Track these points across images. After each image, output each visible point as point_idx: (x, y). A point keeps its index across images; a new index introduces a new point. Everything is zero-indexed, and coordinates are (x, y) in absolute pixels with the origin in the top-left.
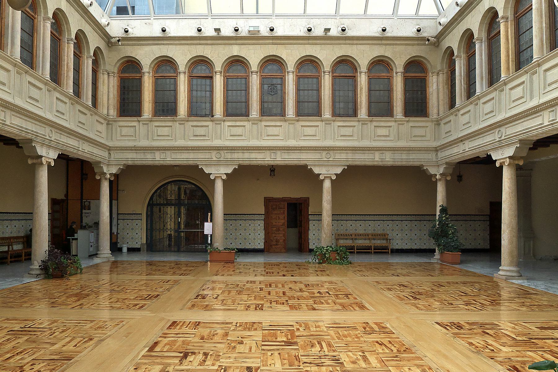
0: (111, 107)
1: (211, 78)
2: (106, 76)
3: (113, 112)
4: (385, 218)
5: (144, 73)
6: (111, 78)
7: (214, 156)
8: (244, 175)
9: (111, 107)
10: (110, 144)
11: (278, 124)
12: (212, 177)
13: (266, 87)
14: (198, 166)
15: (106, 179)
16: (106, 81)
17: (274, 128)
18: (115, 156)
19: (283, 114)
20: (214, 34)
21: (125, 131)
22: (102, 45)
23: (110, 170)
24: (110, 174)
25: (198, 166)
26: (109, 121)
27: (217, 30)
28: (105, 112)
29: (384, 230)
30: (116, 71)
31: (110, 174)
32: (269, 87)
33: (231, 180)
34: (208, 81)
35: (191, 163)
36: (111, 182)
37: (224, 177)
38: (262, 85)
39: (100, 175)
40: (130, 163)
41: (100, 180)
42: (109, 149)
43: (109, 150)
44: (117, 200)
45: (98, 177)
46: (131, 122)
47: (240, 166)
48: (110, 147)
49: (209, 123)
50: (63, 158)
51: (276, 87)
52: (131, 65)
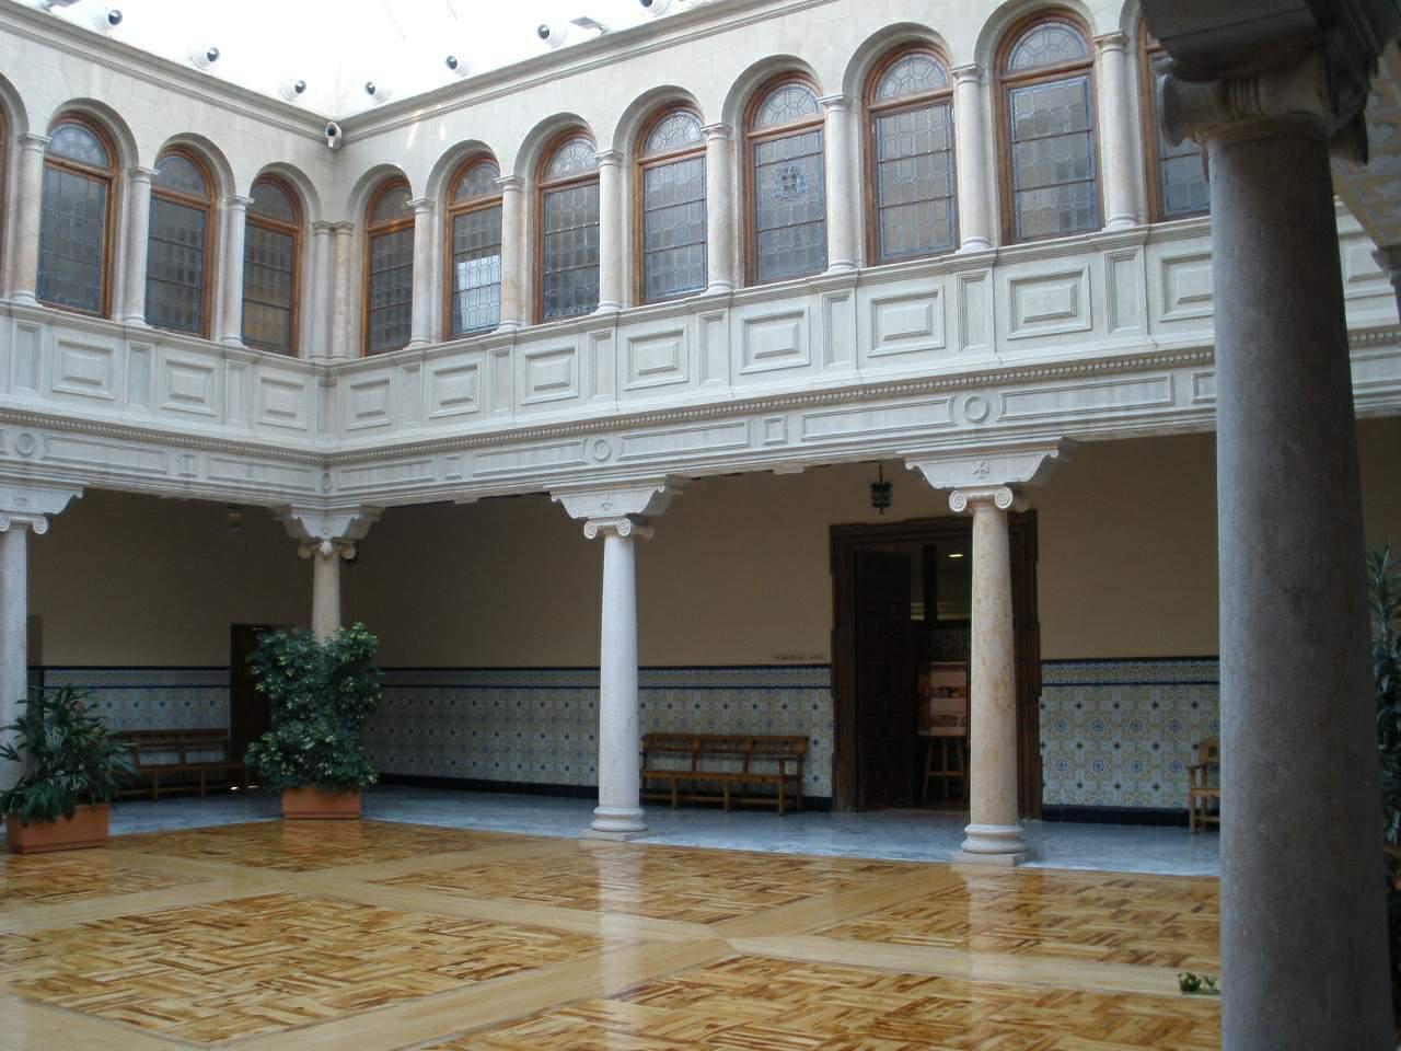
2: (324, 238)
4: (690, 678)
6: (343, 239)
8: (702, 517)
12: (590, 532)
18: (342, 481)
23: (326, 530)
24: (335, 541)
29: (656, 722)
36: (345, 564)
37: (626, 528)
40: (385, 501)
41: (312, 558)
45: (305, 553)
49: (579, 342)
52: (389, 184)
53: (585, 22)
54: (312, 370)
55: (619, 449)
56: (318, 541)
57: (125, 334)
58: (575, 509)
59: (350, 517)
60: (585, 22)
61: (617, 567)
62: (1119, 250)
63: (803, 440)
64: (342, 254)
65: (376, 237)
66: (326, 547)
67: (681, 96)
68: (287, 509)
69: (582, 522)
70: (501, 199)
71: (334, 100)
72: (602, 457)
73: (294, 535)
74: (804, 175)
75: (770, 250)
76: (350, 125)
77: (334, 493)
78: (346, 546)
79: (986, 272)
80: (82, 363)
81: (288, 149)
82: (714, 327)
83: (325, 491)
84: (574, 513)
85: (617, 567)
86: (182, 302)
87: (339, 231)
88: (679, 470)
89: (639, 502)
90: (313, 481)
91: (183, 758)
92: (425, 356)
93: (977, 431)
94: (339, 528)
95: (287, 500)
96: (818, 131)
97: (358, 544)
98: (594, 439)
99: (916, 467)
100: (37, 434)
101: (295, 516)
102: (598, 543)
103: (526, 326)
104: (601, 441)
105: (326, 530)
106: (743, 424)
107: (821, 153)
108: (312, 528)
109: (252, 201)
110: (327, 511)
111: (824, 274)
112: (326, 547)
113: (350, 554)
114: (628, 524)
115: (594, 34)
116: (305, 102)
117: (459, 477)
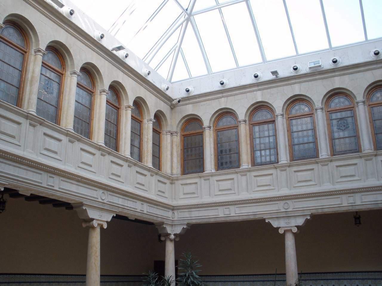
1: (273, 122)
3: (177, 170)
5: (205, 128)
7: (280, 206)
10: (174, 203)
12: (281, 231)
14: (264, 220)
15: (171, 240)
18: (177, 215)
19: (357, 149)
20: (271, 77)
22: (164, 107)
23: (173, 231)
24: (175, 235)
25: (264, 220)
26: (172, 180)
27: (275, 73)
28: (169, 171)
30: (179, 130)
31: (175, 235)
32: (338, 121)
33: (303, 234)
34: (271, 126)
35: (257, 217)
37: (295, 230)
38: (329, 120)
40: (194, 222)
42: (173, 208)
43: (173, 210)
46: (192, 179)
47: (313, 216)
48: (174, 207)
50: (120, 219)
51: (346, 120)
55: (293, 205)
56: (170, 234)
58: (275, 224)
59: (182, 227)
61: (290, 243)
62: (325, 162)
63: (348, 203)
65: (185, 137)
68: (163, 223)
69: (278, 228)
71: (177, 94)
72: (286, 208)
73: (160, 232)
75: (227, 160)
79: (373, 158)
81: (164, 107)
83: (173, 218)
84: (275, 226)
85: (290, 243)
87: (173, 134)
88: (190, 222)
92: (212, 175)
93: (286, 212)
94: (178, 230)
95: (164, 221)
96: (201, 134)
99: (269, 222)
101: (165, 226)
102: (283, 236)
103: (213, 171)
104: (287, 203)
108: (169, 230)
109: (155, 121)
110: (172, 225)
111: (204, 173)
112: (172, 237)
113: (177, 240)
116: (168, 93)
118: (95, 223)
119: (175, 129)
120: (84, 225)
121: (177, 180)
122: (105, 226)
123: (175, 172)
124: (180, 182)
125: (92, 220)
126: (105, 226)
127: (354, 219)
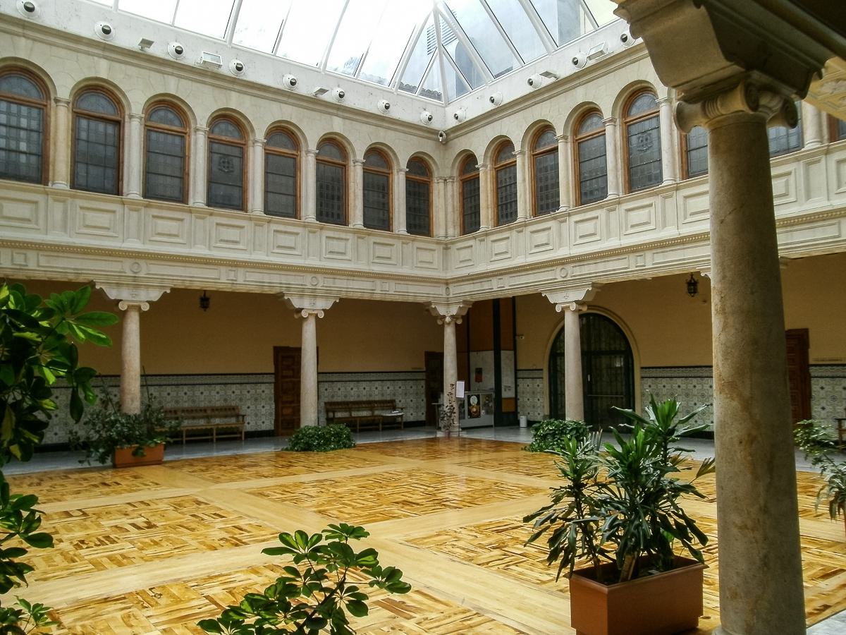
0: (450, 224)
2: (442, 185)
3: (454, 231)
6: (449, 186)
9: (450, 224)
10: (449, 275)
11: (646, 201)
12: (558, 309)
13: (634, 140)
16: (442, 193)
17: (642, 212)
18: (455, 290)
21: (465, 254)
23: (449, 311)
24: (452, 317)
26: (446, 244)
30: (456, 173)
39: (441, 319)
42: (447, 283)
43: (447, 284)
44: (515, 349)
45: (439, 322)
53: (547, 74)
54: (438, 243)
57: (399, 237)
60: (547, 74)
63: (653, 264)
64: (449, 194)
66: (448, 319)
67: (591, 106)
68: (430, 303)
70: (516, 161)
73: (434, 314)
74: (650, 139)
76: (448, 132)
77: (451, 296)
78: (457, 319)
80: (336, 245)
82: (612, 214)
86: (378, 218)
89: (580, 295)
90: (441, 290)
91: (373, 413)
92: (487, 234)
94: (454, 310)
97: (463, 317)
98: (560, 267)
100: (319, 276)
105: (449, 311)
106: (625, 258)
107: (658, 128)
108: (442, 311)
114: (574, 304)
115: (552, 80)
117: (503, 287)
118: (304, 314)
119: (447, 173)
120: (296, 316)
121: (453, 243)
122: (321, 315)
123: (451, 231)
124: (460, 245)
125: (300, 310)
126: (321, 315)
127: (686, 285)
